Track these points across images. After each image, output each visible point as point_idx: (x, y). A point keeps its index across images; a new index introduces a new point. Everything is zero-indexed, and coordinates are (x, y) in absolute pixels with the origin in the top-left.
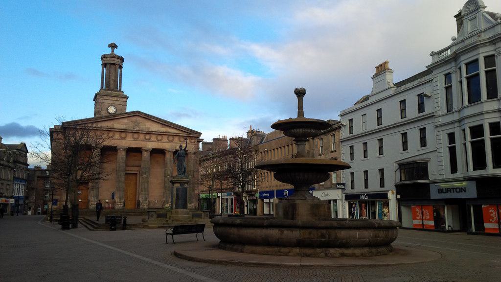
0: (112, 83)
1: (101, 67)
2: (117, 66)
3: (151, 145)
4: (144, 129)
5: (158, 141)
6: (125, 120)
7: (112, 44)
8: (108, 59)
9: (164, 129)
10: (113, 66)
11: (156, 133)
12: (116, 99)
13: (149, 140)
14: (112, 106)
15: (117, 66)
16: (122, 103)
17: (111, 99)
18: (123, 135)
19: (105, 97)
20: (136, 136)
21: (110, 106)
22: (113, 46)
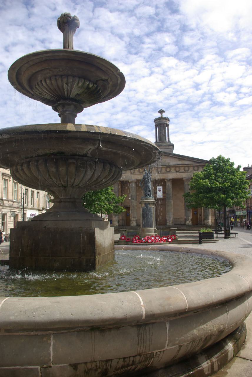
3: (171, 176)
5: (177, 172)
8: (158, 121)
10: (162, 126)
12: (165, 147)
13: (169, 172)
16: (169, 150)
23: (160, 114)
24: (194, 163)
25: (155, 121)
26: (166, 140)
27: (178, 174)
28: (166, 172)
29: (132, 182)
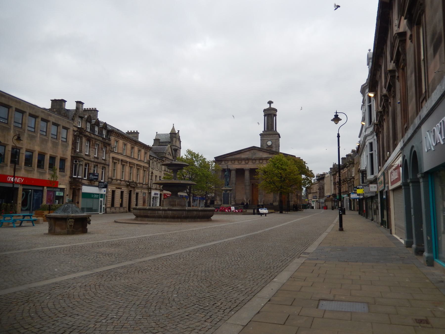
1: (263, 117)
6: (248, 153)
7: (269, 101)
8: (266, 111)
12: (271, 136)
14: (269, 141)
15: (273, 115)
17: (268, 136)
18: (247, 162)
19: (265, 136)
20: (254, 161)
21: (268, 141)
22: (270, 103)
25: (264, 112)
29: (232, 170)
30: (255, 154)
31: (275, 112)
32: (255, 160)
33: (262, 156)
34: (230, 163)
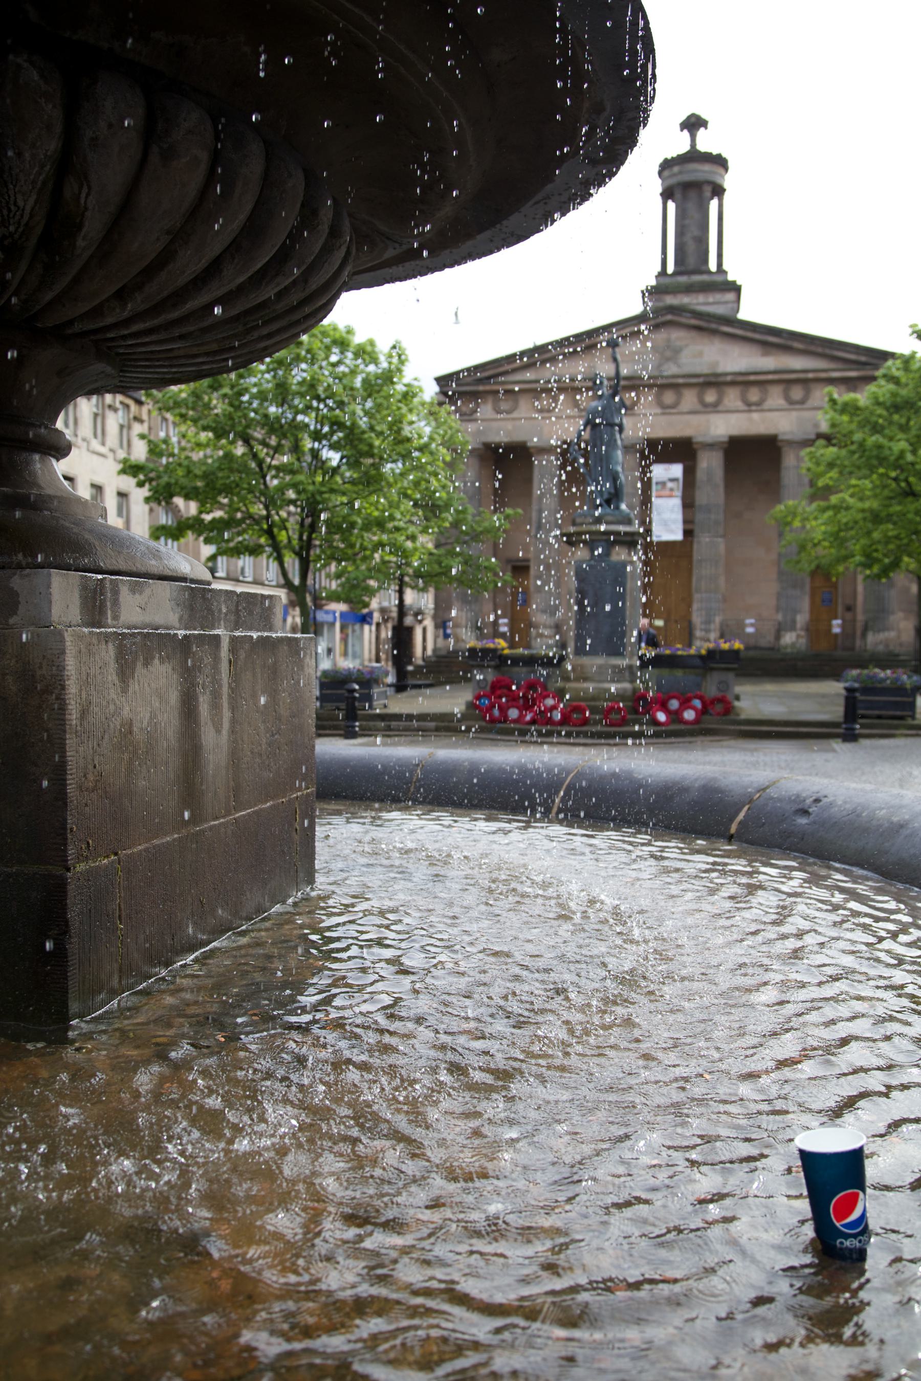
0: (691, 247)
1: (659, 200)
2: (707, 190)
4: (698, 370)
5: (750, 406)
8: (676, 169)
9: (797, 363)
10: (693, 194)
11: (740, 378)
13: (714, 408)
15: (707, 190)
23: (686, 131)
24: (832, 365)
25: (660, 173)
26: (706, 260)
27: (755, 416)
28: (699, 407)
30: (677, 351)
31: (722, 171)
32: (675, 387)
33: (717, 364)
34: (525, 409)
